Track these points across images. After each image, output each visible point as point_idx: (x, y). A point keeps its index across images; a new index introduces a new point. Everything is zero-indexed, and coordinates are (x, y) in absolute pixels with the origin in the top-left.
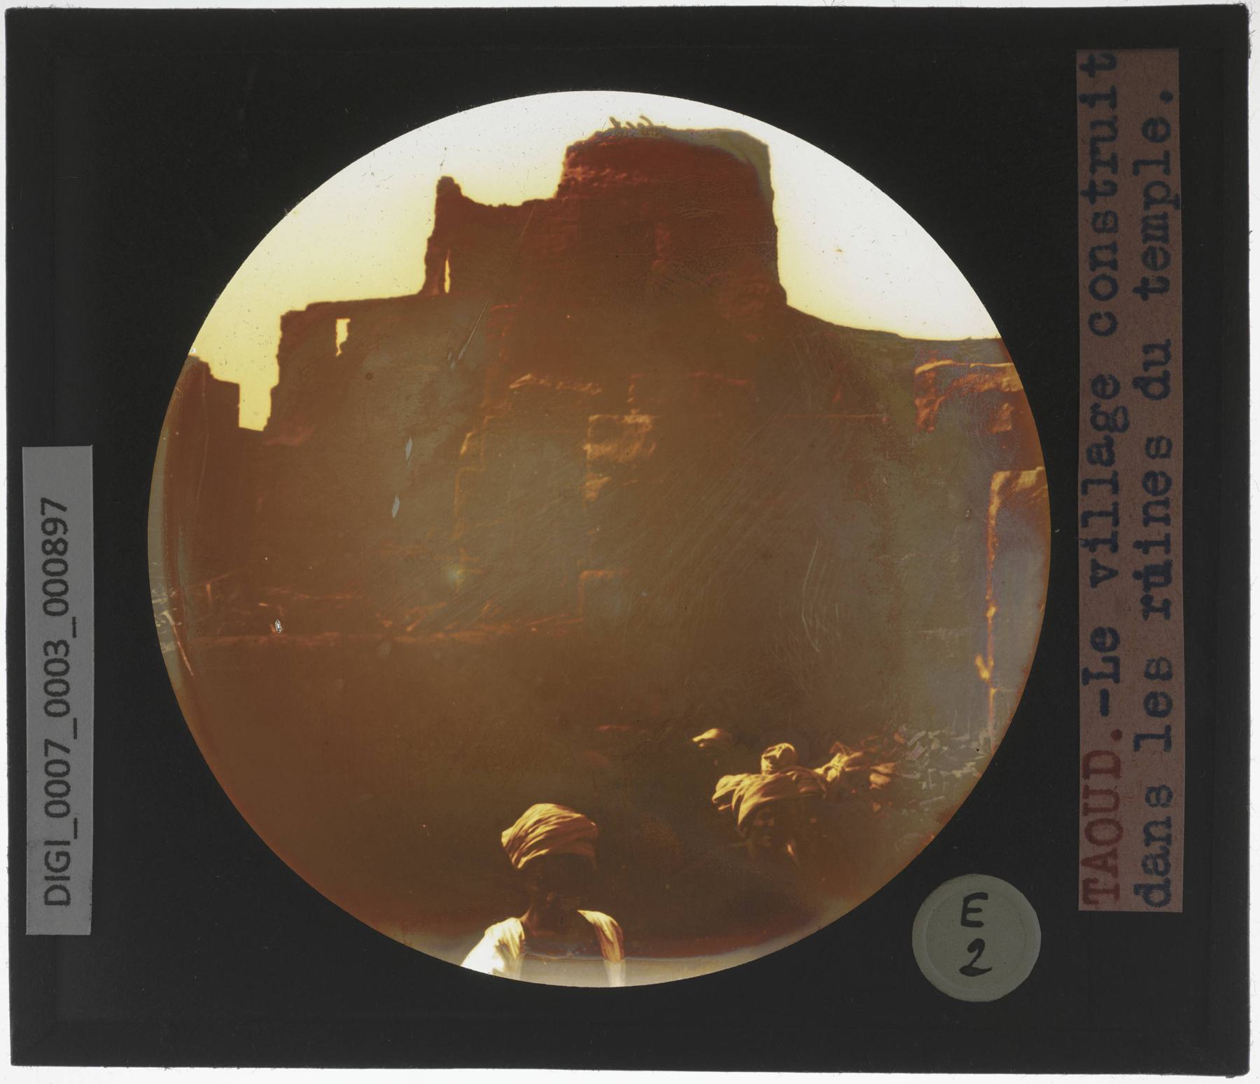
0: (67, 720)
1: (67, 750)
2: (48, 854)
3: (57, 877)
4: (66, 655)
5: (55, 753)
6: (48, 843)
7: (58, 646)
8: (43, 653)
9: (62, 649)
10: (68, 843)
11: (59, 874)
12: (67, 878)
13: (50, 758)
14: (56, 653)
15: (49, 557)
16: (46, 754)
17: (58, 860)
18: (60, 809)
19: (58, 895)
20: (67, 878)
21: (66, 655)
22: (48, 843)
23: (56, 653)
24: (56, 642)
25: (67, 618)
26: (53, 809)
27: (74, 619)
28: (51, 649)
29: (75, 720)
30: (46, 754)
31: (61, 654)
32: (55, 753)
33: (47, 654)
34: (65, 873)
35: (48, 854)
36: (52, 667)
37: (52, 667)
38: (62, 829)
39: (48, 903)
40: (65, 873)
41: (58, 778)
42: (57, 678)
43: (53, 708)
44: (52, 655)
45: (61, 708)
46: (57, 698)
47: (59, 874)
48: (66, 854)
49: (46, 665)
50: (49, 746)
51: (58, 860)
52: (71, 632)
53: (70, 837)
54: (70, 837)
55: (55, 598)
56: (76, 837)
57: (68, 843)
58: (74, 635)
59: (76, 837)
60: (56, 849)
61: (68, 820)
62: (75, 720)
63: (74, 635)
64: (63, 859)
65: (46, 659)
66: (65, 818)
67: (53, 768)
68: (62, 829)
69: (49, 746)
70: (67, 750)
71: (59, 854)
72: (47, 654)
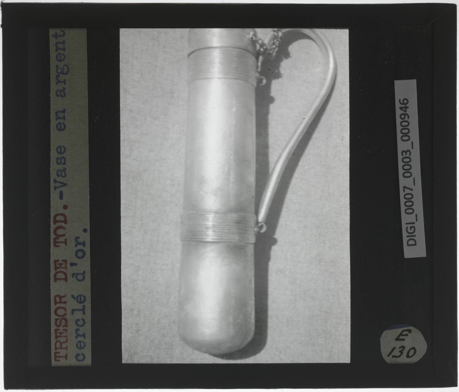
0: (411, 179)
1: (412, 190)
2: (407, 227)
3: (411, 236)
4: (410, 155)
5: (407, 191)
6: (407, 224)
7: (407, 152)
8: (401, 155)
9: (408, 153)
10: (414, 223)
11: (410, 235)
12: (415, 236)
13: (405, 193)
14: (406, 154)
15: (402, 120)
16: (404, 191)
17: (411, 229)
18: (411, 211)
19: (411, 242)
20: (415, 236)
21: (410, 155)
22: (407, 224)
23: (406, 154)
24: (406, 150)
25: (409, 142)
26: (408, 211)
27: (412, 143)
28: (404, 154)
29: (414, 179)
30: (404, 191)
31: (408, 155)
32: (407, 191)
33: (403, 155)
34: (413, 234)
35: (407, 227)
36: (406, 160)
37: (406, 160)
38: (411, 218)
39: (408, 245)
40: (413, 234)
41: (409, 200)
42: (407, 164)
43: (406, 175)
44: (405, 156)
45: (408, 175)
46: (407, 171)
47: (410, 235)
48: (414, 227)
49: (403, 159)
50: (406, 189)
51: (411, 229)
52: (411, 148)
53: (415, 221)
54: (415, 221)
55: (405, 135)
56: (417, 220)
57: (414, 223)
58: (412, 148)
59: (417, 220)
60: (409, 226)
61: (414, 215)
62: (414, 179)
63: (412, 148)
64: (413, 229)
65: (404, 157)
66: (412, 215)
67: (408, 196)
68: (411, 218)
69: (406, 189)
70: (412, 190)
71: (411, 227)
72: (403, 155)
